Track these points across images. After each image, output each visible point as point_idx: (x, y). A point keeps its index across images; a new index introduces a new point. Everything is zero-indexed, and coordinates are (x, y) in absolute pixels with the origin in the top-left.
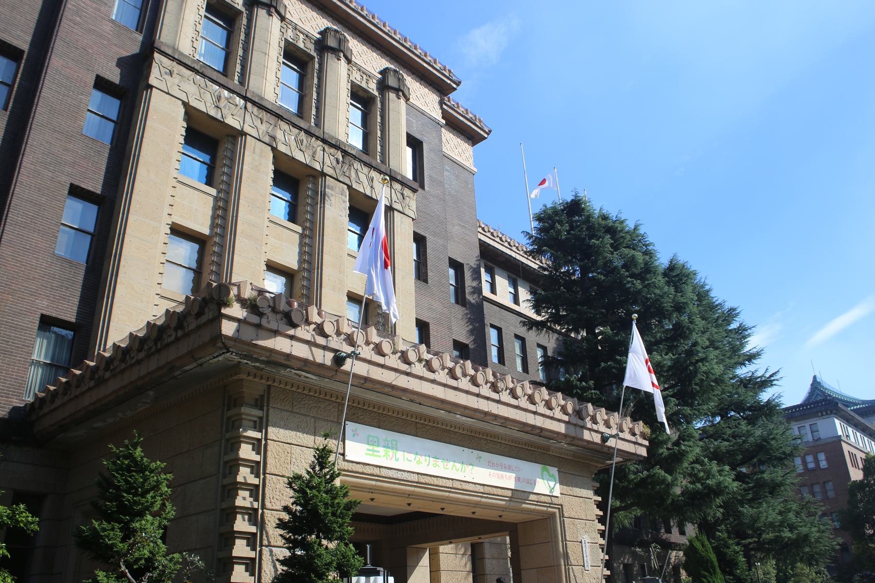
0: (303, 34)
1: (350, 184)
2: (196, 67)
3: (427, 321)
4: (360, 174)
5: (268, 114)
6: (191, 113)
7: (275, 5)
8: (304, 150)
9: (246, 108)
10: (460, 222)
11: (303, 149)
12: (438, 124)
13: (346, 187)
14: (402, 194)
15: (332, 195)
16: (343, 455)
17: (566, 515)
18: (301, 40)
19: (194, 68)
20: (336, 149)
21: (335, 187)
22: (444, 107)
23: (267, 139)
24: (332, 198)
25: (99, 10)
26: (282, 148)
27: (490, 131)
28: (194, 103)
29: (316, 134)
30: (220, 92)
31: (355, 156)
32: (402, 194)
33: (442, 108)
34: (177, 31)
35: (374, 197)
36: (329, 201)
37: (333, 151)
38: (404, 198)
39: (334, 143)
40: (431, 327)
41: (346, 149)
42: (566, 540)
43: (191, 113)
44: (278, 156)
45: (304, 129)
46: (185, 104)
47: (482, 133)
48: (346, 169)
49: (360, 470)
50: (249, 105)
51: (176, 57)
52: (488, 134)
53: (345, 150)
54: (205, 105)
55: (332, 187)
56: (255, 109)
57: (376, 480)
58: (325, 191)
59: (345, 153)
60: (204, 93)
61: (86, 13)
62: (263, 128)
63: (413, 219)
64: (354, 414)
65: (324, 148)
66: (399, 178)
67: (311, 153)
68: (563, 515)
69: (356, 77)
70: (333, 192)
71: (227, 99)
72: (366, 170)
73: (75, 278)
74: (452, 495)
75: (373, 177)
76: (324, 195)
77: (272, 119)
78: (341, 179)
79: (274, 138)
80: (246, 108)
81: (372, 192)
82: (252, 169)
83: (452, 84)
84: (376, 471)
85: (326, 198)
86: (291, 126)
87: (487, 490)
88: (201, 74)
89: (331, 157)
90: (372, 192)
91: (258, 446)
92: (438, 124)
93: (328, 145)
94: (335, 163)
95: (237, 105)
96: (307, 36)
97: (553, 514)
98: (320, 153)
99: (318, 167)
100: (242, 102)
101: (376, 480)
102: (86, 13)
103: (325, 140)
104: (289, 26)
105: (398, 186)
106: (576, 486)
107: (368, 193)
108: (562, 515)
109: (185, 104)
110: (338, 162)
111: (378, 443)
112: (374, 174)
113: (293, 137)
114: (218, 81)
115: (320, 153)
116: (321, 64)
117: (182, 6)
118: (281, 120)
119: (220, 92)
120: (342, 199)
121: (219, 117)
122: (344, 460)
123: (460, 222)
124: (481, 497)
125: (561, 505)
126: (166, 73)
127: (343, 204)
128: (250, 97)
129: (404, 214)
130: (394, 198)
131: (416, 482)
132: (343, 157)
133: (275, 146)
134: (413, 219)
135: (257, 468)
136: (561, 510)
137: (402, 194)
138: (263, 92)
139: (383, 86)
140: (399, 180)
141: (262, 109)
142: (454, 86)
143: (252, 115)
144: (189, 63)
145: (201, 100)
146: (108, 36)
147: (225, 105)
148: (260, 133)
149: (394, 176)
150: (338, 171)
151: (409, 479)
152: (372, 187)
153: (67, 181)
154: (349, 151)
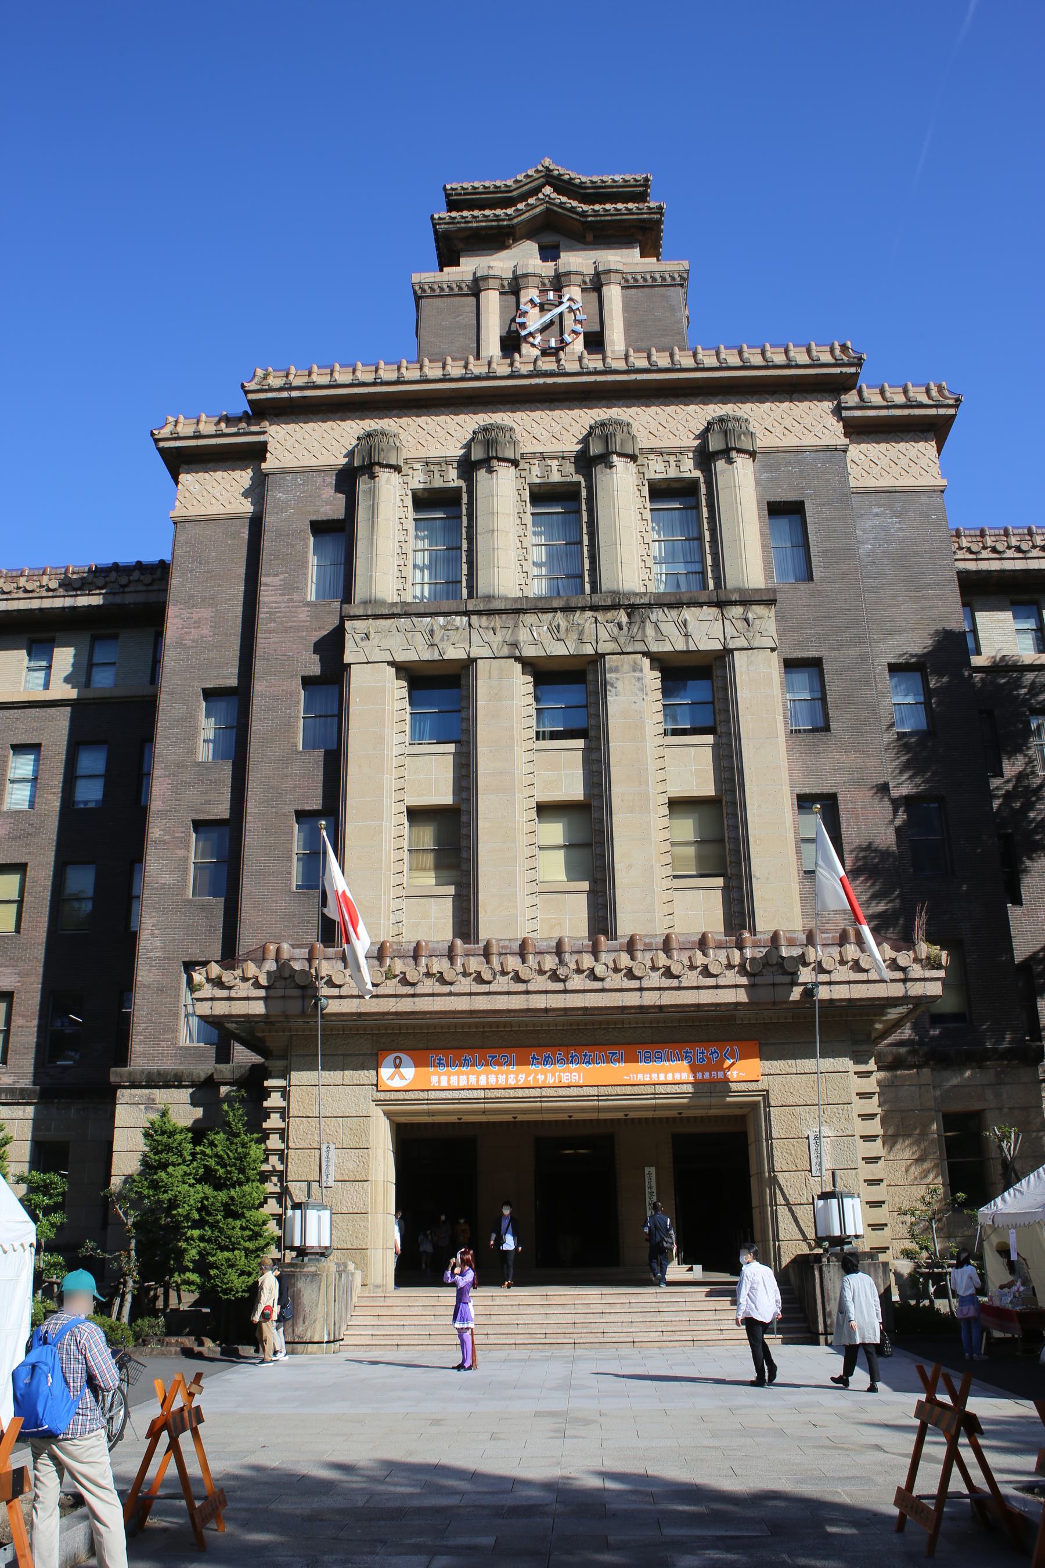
0: (556, 458)
1: (646, 649)
2: (395, 612)
3: (831, 791)
4: (662, 626)
5: (504, 616)
6: (403, 669)
7: (494, 455)
8: (563, 637)
9: (470, 625)
10: (913, 594)
11: (562, 635)
12: (836, 450)
13: (640, 656)
14: (746, 620)
15: (617, 679)
16: (376, 1085)
17: (773, 1103)
18: (555, 469)
19: (393, 614)
20: (615, 609)
21: (622, 665)
22: (845, 413)
23: (505, 651)
24: (619, 685)
25: (292, 600)
26: (530, 651)
27: (958, 400)
28: (400, 657)
29: (580, 605)
30: (432, 625)
31: (650, 604)
32: (745, 619)
33: (841, 418)
34: (371, 576)
35: (692, 648)
36: (613, 690)
37: (610, 615)
38: (749, 625)
39: (610, 604)
40: (840, 798)
41: (631, 602)
42: (771, 1139)
43: (403, 669)
44: (529, 665)
45: (560, 608)
46: (391, 664)
47: (942, 411)
48: (635, 630)
49: (401, 1097)
50: (474, 619)
51: (369, 613)
52: (956, 406)
53: (629, 605)
54: (418, 652)
55: (617, 667)
56: (484, 621)
57: (428, 1104)
58: (605, 679)
59: (632, 609)
60: (413, 636)
61: (279, 612)
62: (496, 640)
63: (773, 650)
64: (393, 1041)
65: (596, 618)
66: (735, 597)
67: (576, 637)
68: (769, 1103)
69: (658, 469)
70: (618, 675)
71: (444, 628)
72: (674, 613)
74: (544, 1104)
75: (686, 620)
76: (605, 684)
77: (509, 620)
78: (630, 650)
79: (515, 645)
80: (470, 625)
81: (687, 643)
82: (490, 700)
83: (845, 370)
84: (425, 1095)
85: (608, 687)
86: (540, 615)
87: (603, 1091)
88: (405, 614)
89: (608, 625)
90: (687, 643)
91: (285, 1094)
92: (836, 450)
93: (603, 610)
94: (616, 630)
95: (458, 628)
96: (563, 458)
97: (756, 1104)
98: (589, 627)
99: (589, 650)
100: (465, 619)
101: (428, 1104)
102: (279, 612)
103: (596, 606)
104: (532, 461)
105: (737, 611)
106: (795, 1057)
107: (680, 646)
108: (767, 1105)
109: (391, 664)
110: (620, 627)
111: (447, 1062)
112: (688, 614)
113: (545, 628)
114: (427, 611)
115: (589, 627)
116: (590, 488)
117: (372, 539)
118: (524, 613)
119: (432, 625)
120: (634, 677)
121: (436, 656)
122: (378, 1091)
123: (913, 594)
124: (598, 1100)
125: (767, 1091)
126: (362, 639)
127: (638, 685)
128: (471, 609)
129: (752, 649)
130: (730, 630)
131: (484, 1099)
132: (629, 615)
133: (518, 654)
134: (773, 650)
135: (284, 1113)
136: (766, 1097)
137: (746, 620)
138: (496, 587)
139: (705, 458)
140: (736, 601)
141: (493, 614)
142: (853, 370)
143: (481, 630)
144: (386, 611)
145: (409, 647)
146: (305, 624)
147: (443, 637)
148: (495, 647)
149: (724, 599)
150: (622, 640)
151: (469, 1096)
152: (686, 635)
153: (290, 809)
154: (638, 602)
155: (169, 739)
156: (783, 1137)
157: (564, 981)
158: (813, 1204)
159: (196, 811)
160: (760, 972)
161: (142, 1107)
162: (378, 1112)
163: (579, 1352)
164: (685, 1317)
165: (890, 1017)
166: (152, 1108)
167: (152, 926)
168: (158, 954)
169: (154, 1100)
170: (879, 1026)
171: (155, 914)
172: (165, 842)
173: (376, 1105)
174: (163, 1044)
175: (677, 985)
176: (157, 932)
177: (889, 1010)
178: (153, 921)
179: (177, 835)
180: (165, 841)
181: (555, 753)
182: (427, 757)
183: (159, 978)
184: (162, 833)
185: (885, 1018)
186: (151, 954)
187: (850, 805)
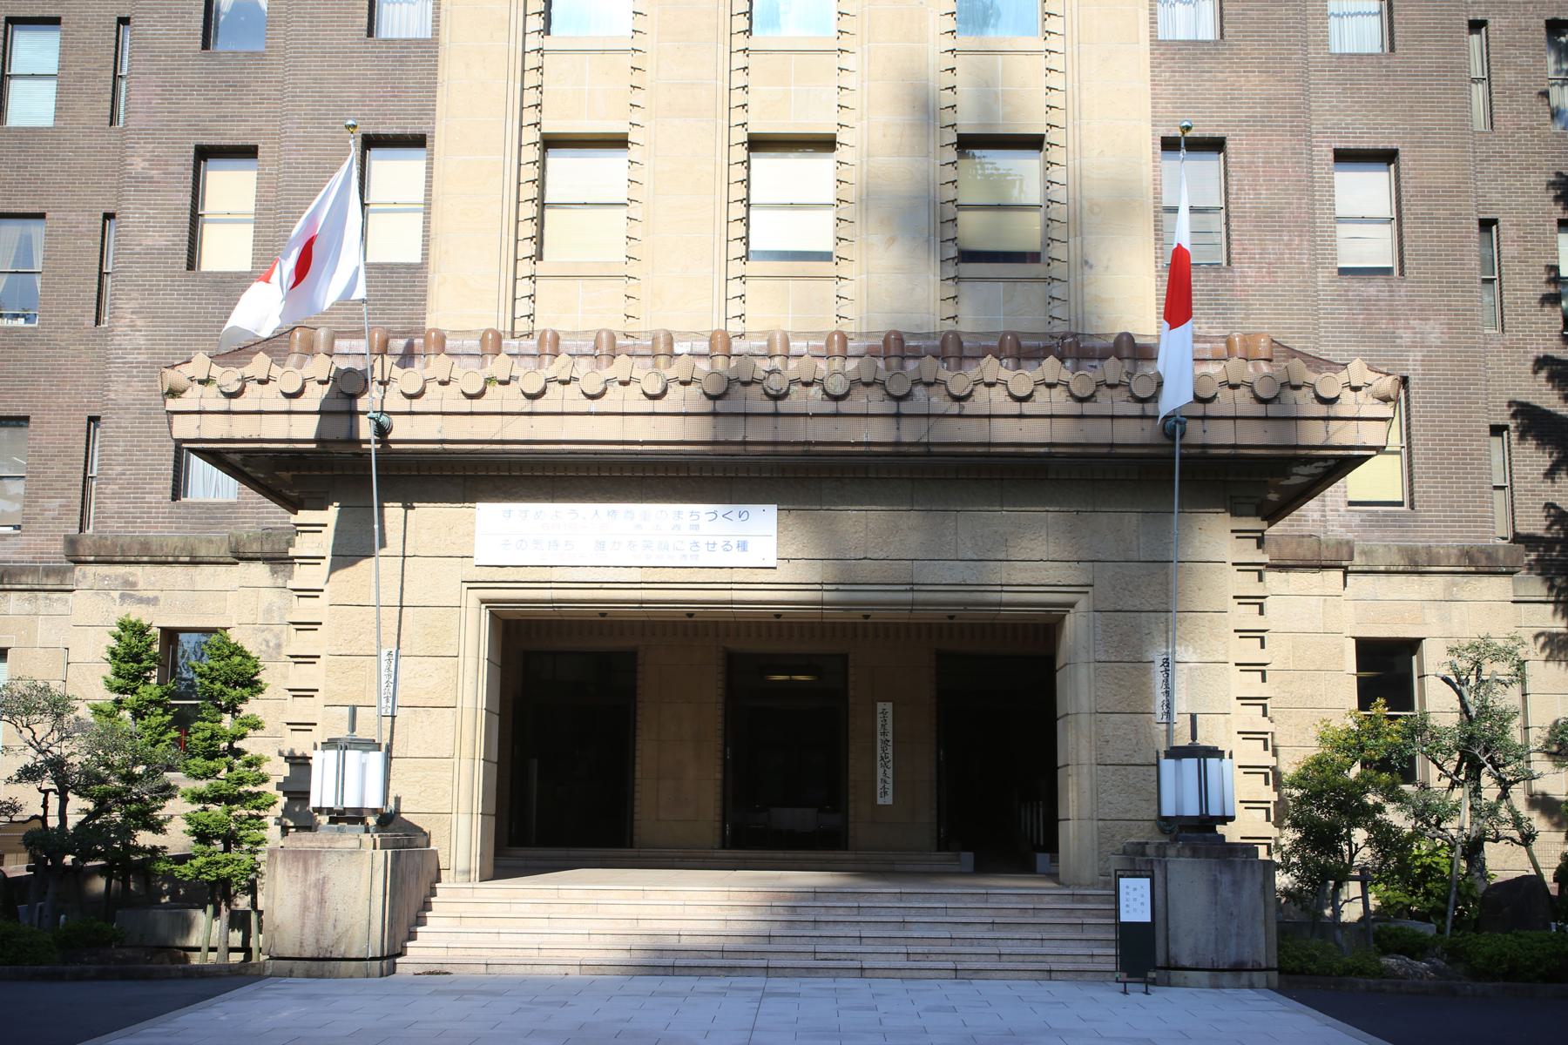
3: (1217, 134)
73: (393, 291)
155: (155, 11)
156: (1113, 659)
158: (1158, 765)
159: (205, 131)
160: (1092, 396)
161: (116, 594)
163: (776, 983)
164: (943, 932)
165: (1294, 480)
166: (131, 596)
167: (133, 313)
168: (142, 358)
169: (133, 585)
170: (1273, 497)
171: (134, 295)
172: (151, 180)
174: (149, 498)
175: (956, 412)
176: (139, 323)
177: (1295, 470)
178: (133, 304)
179: (171, 169)
180: (152, 178)
181: (782, 56)
182: (576, 56)
183: (142, 395)
184: (146, 164)
185: (1286, 482)
186: (130, 358)
187: (1246, 158)
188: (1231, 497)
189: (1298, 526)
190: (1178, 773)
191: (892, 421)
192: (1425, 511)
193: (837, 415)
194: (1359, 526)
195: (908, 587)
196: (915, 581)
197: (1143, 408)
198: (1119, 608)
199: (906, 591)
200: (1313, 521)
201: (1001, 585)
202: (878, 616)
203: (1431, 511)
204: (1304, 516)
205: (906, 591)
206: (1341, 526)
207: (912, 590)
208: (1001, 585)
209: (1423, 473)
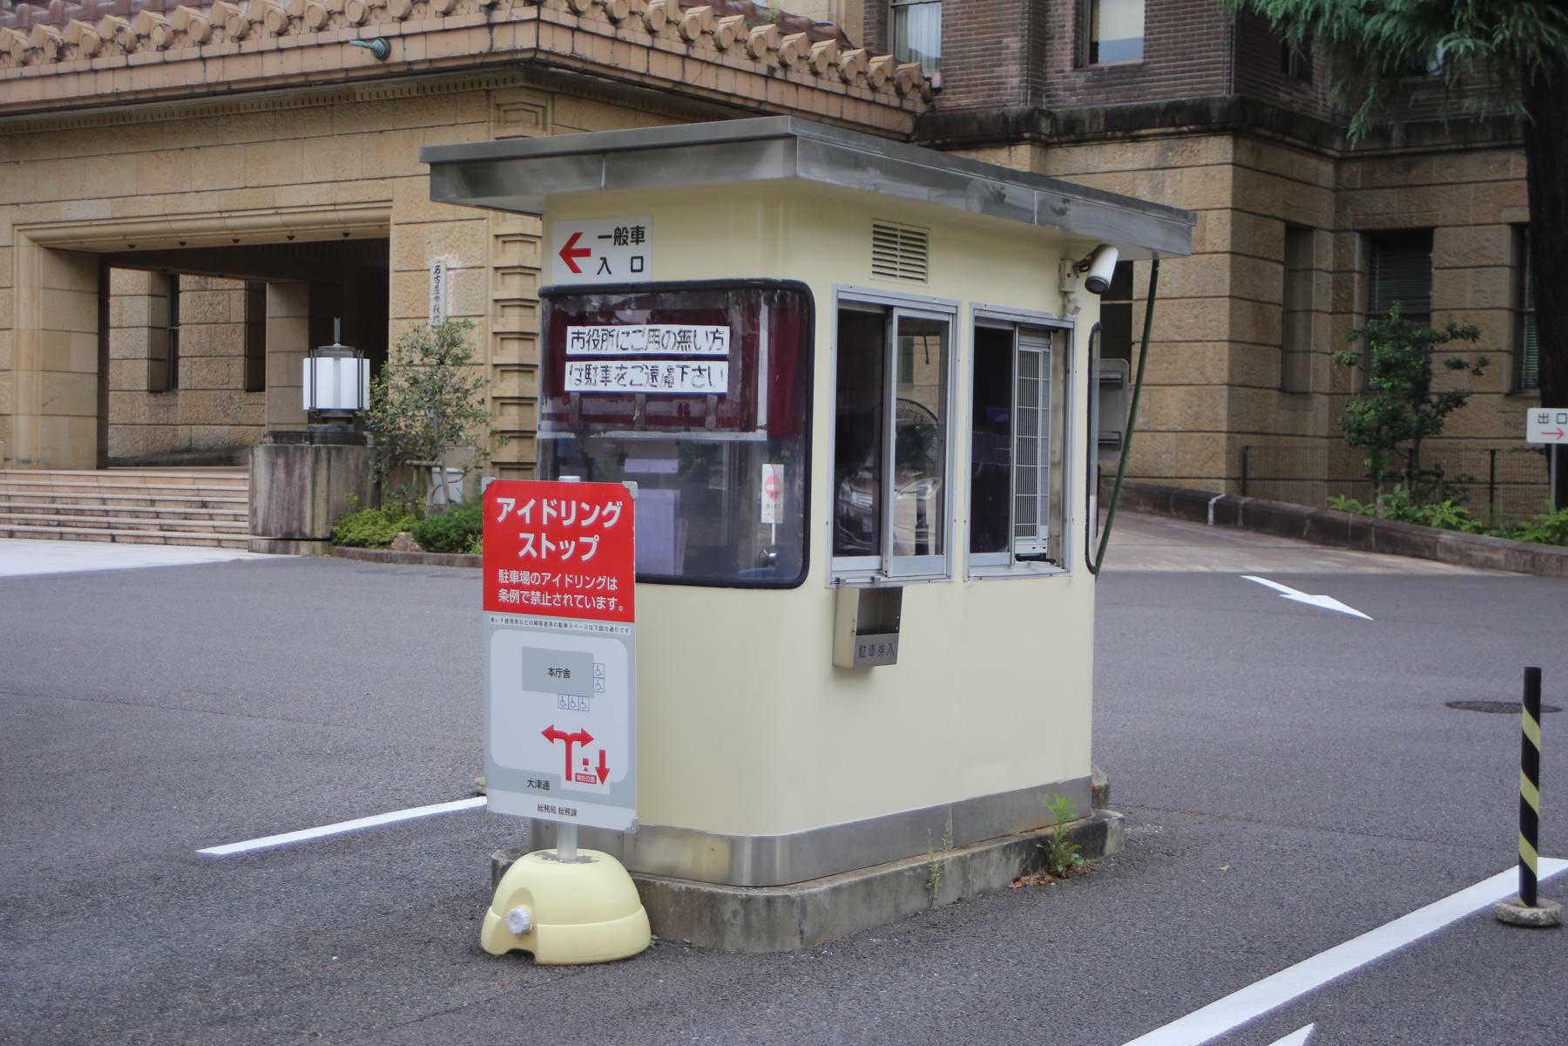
157: (129, 51)
162: (23, 239)
173: (19, 230)
188: (498, 105)
189: (997, 95)
190: (338, 373)
191: (200, 65)
192: (1154, 63)
193: (165, 63)
194: (1086, 88)
195: (274, 211)
196: (277, 205)
197: (358, 33)
198: (408, 220)
199: (274, 214)
200: (1012, 88)
201: (335, 205)
202: (246, 240)
203: (1159, 62)
204: (1003, 83)
205: (274, 214)
206: (1065, 90)
207: (277, 214)
208: (335, 205)
209: (1156, 16)
